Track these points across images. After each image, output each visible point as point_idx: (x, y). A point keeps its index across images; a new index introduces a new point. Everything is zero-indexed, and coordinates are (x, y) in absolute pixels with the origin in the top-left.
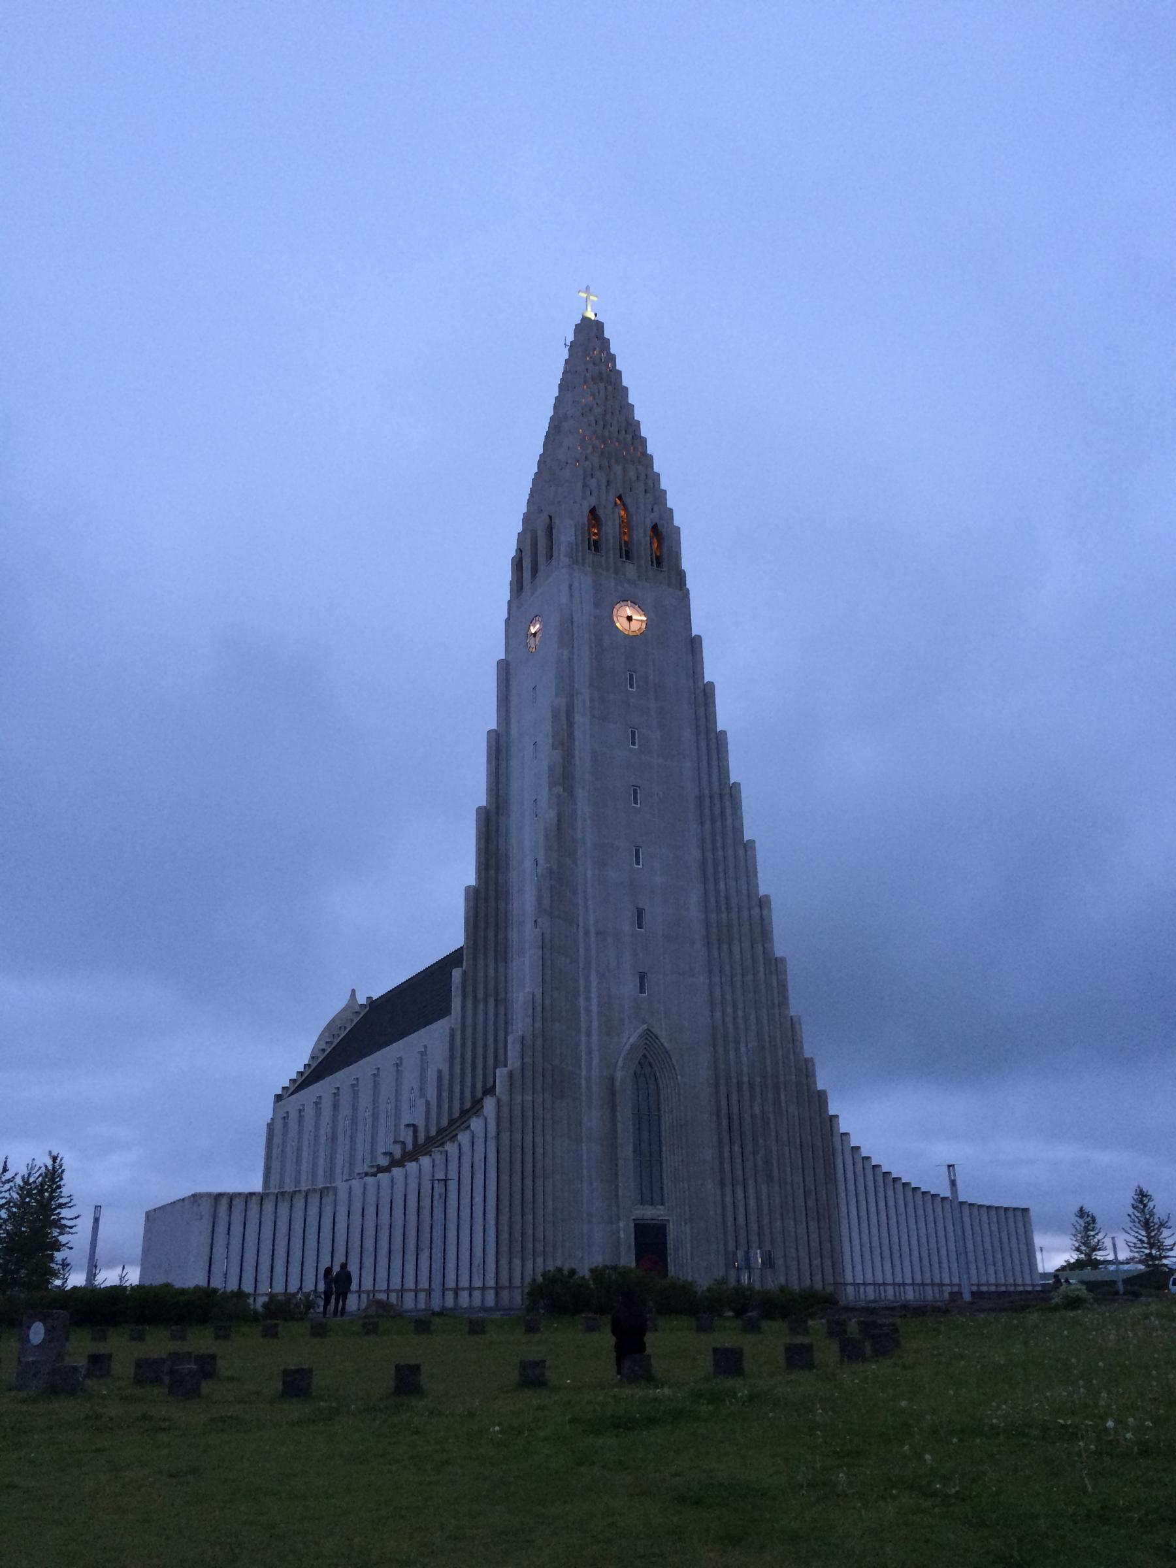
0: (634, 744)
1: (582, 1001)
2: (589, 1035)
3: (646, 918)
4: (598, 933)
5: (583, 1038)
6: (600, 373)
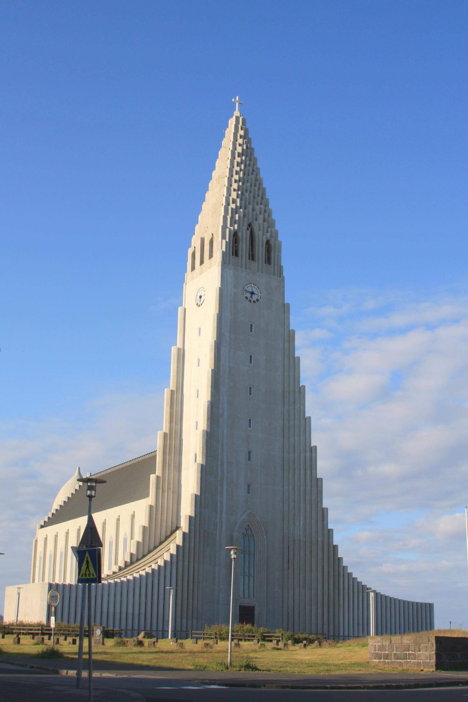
0: (251, 362)
1: (218, 498)
2: (221, 514)
3: (252, 455)
5: (219, 516)
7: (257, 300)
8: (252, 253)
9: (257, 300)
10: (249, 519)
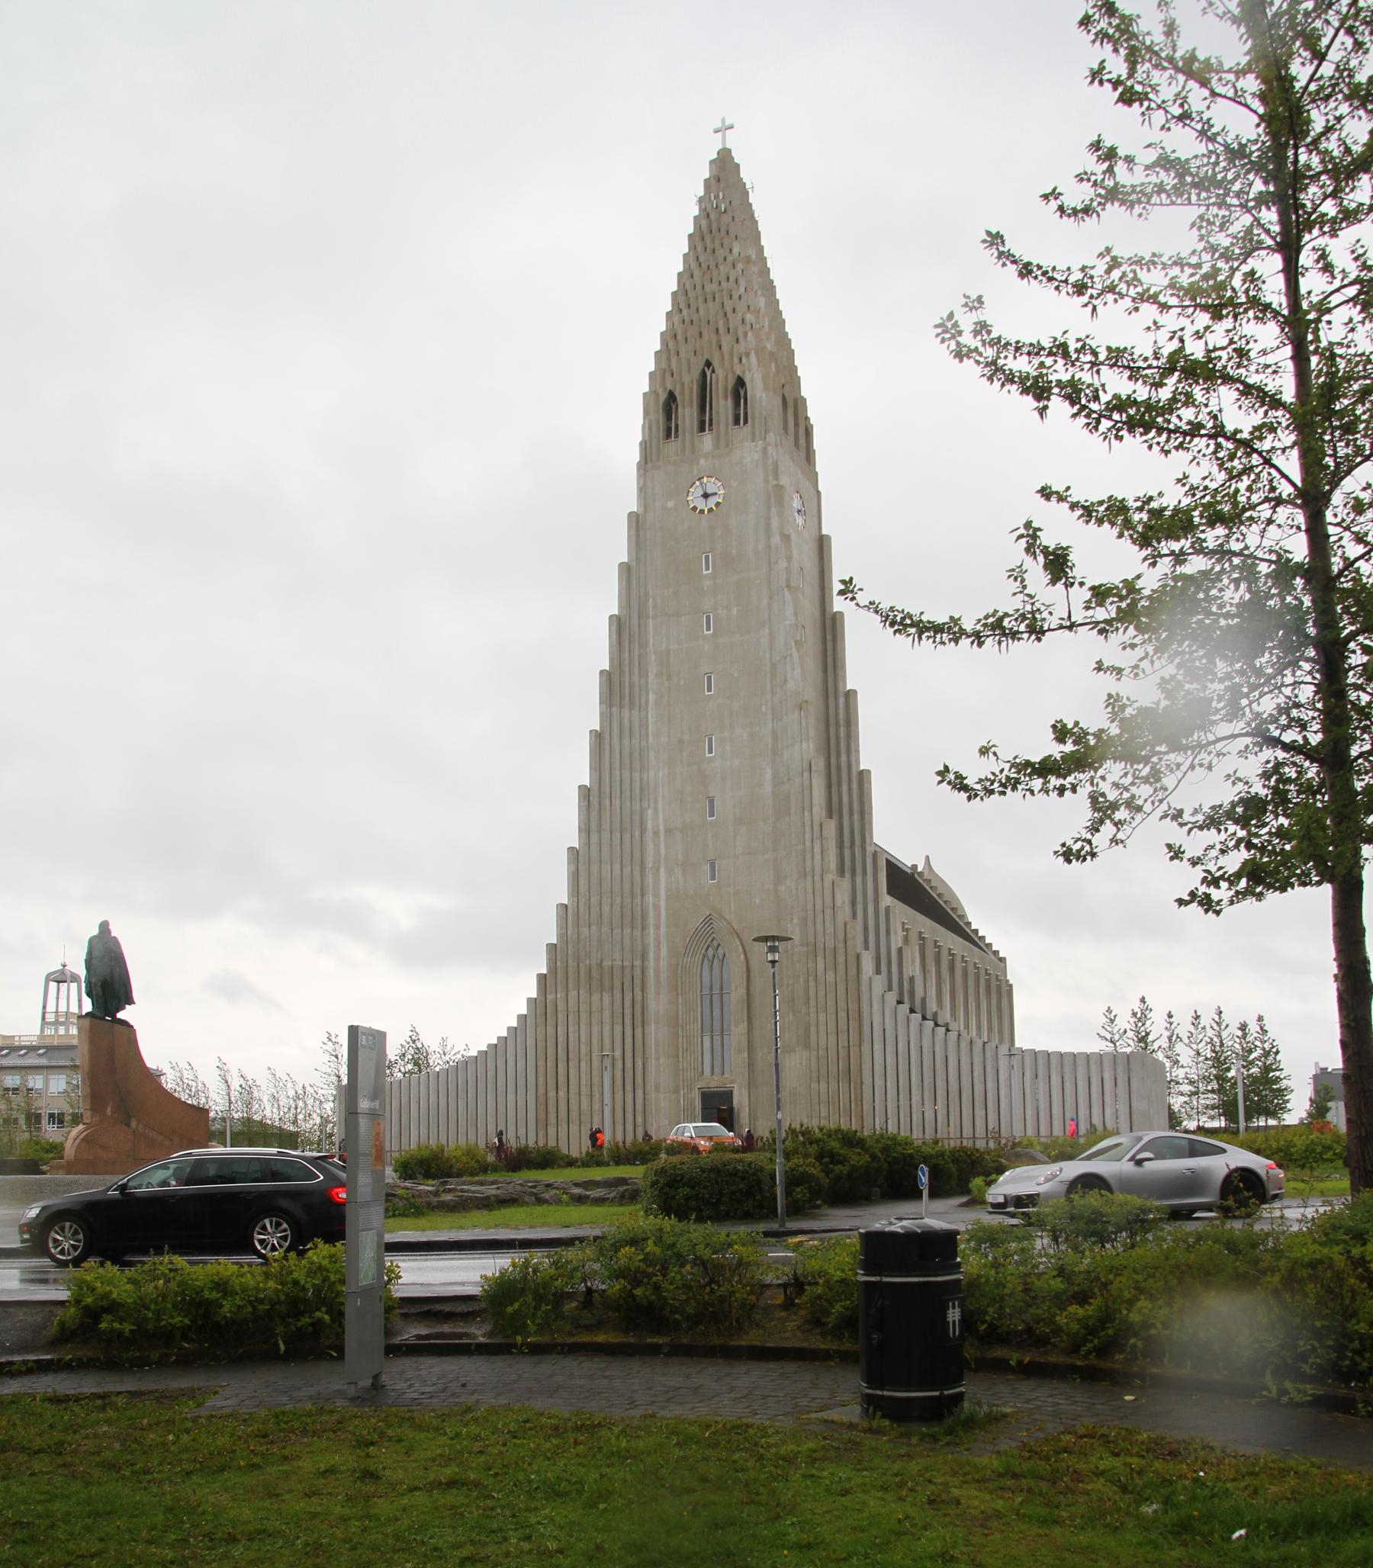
1: (650, 899)
2: (657, 927)
4: (669, 831)
5: (652, 931)
6: (710, 225)
7: (718, 504)
9: (718, 504)
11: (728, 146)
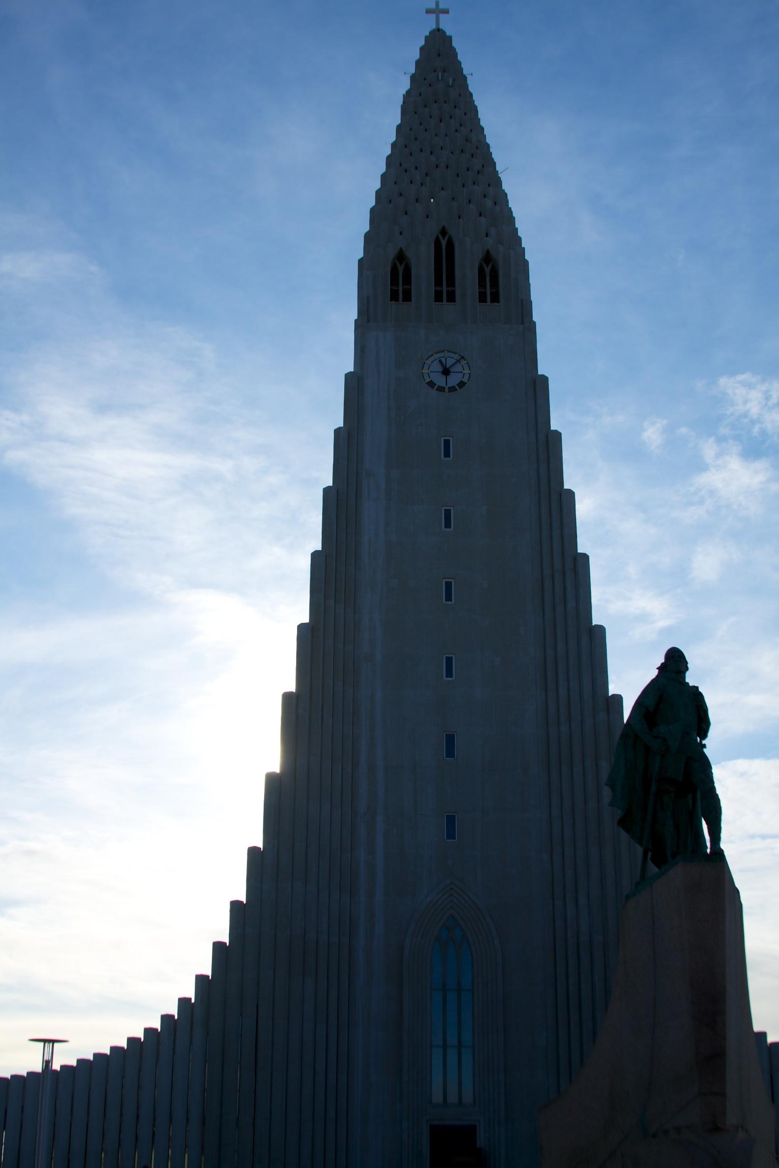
0: (448, 525)
7: (462, 384)
8: (450, 289)
10: (452, 901)
11: (441, 27)
